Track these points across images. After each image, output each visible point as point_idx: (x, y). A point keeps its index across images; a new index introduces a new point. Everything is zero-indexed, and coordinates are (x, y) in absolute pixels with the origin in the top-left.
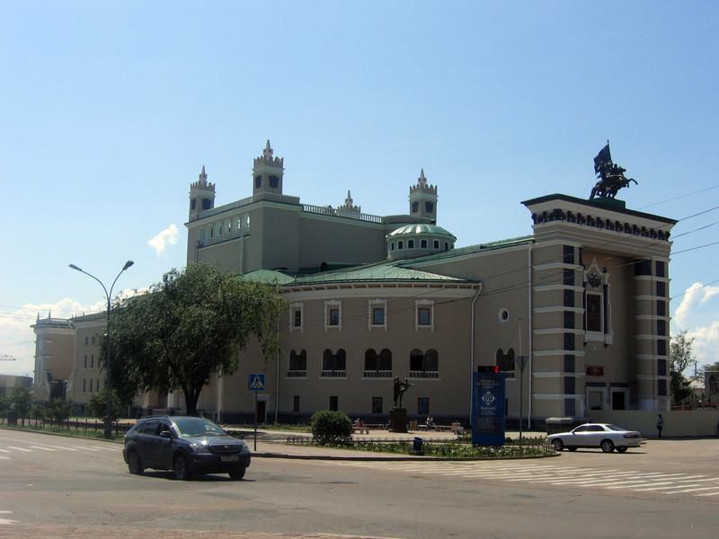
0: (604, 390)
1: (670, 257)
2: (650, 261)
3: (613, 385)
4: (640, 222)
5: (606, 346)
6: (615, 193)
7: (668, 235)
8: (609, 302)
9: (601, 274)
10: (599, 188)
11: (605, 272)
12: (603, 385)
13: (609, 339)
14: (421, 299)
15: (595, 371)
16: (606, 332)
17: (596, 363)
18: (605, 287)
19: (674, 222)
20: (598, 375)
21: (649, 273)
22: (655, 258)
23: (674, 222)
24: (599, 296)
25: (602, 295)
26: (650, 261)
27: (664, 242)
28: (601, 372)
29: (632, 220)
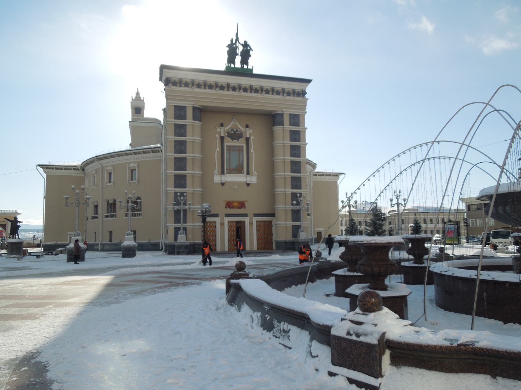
0: (247, 220)
1: (306, 110)
2: (282, 115)
3: (256, 215)
4: (268, 84)
5: (248, 185)
6: (247, 65)
7: (304, 93)
8: (252, 151)
9: (243, 129)
10: (231, 59)
11: (247, 126)
12: (246, 215)
13: (253, 179)
14: (129, 163)
15: (236, 204)
16: (248, 173)
17: (236, 197)
18: (248, 140)
19: (309, 81)
20: (239, 208)
21: (282, 124)
22: (287, 112)
23: (309, 81)
24: (243, 147)
25: (245, 145)
26: (282, 115)
27: (300, 99)
28: (242, 205)
29: (256, 83)
